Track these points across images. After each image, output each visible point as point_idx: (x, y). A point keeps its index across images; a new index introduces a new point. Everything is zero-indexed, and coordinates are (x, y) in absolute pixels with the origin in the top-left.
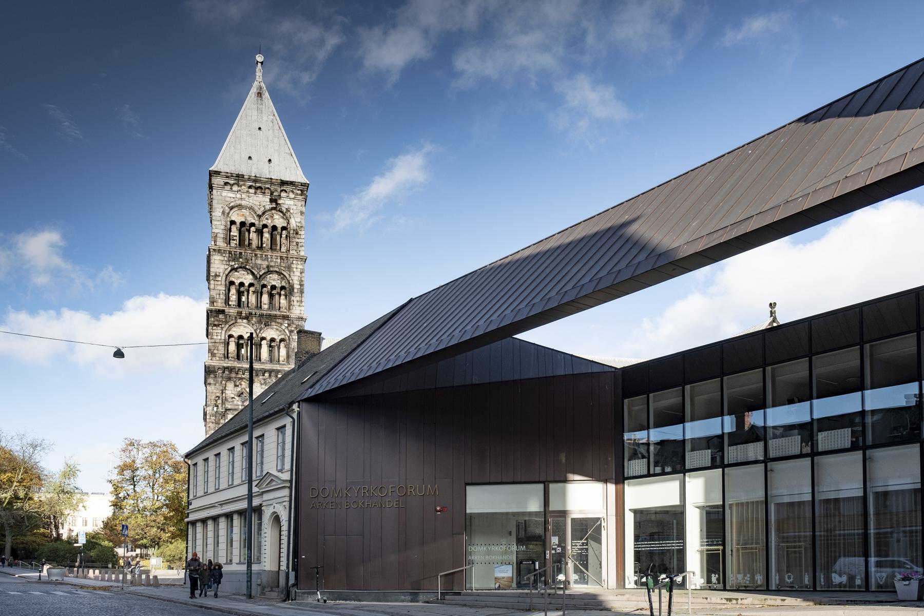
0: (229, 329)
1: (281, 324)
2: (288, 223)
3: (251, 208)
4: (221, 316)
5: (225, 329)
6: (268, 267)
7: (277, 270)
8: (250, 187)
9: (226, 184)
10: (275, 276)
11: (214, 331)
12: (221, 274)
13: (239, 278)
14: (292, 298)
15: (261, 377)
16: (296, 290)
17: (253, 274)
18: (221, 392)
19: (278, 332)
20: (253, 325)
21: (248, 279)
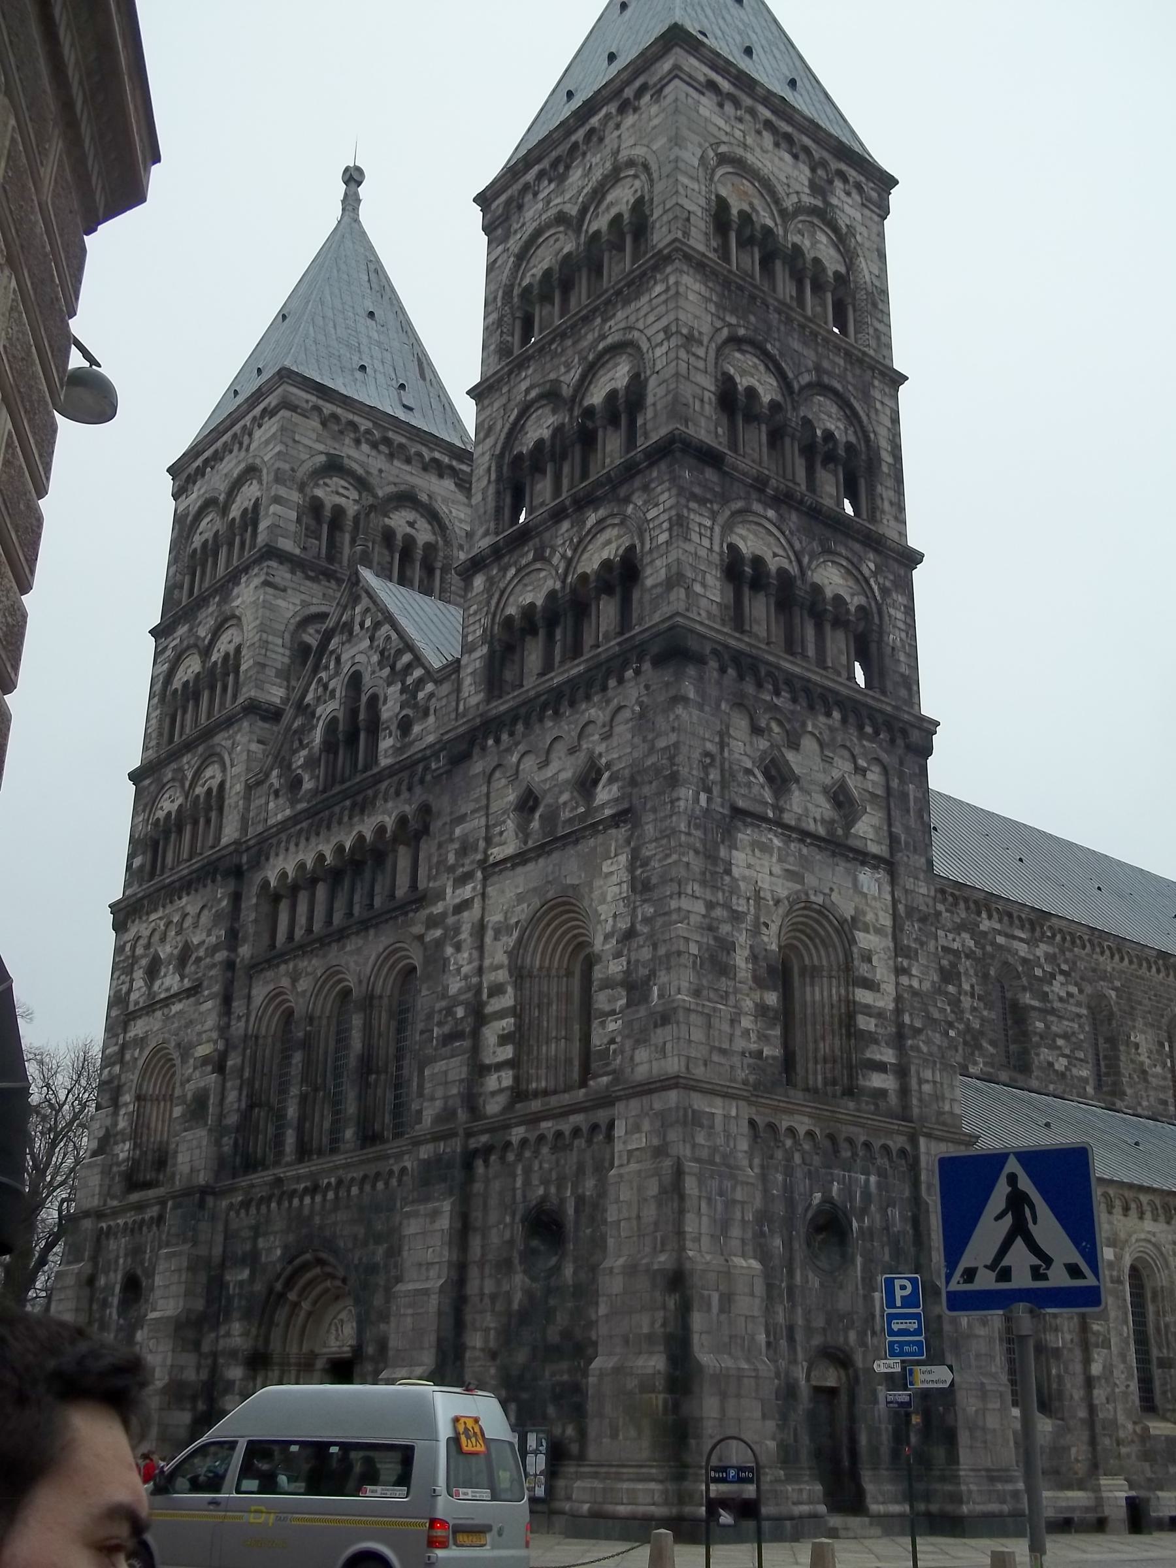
0: (728, 528)
1: (860, 559)
2: (850, 265)
3: (766, 186)
4: (710, 474)
5: (721, 520)
6: (818, 368)
7: (839, 387)
8: (768, 124)
9: (712, 85)
10: (834, 409)
11: (692, 516)
12: (705, 340)
13: (743, 373)
14: (879, 489)
15: (822, 719)
16: (885, 469)
17: (781, 375)
18: (717, 739)
19: (851, 583)
20: (791, 532)
21: (767, 390)
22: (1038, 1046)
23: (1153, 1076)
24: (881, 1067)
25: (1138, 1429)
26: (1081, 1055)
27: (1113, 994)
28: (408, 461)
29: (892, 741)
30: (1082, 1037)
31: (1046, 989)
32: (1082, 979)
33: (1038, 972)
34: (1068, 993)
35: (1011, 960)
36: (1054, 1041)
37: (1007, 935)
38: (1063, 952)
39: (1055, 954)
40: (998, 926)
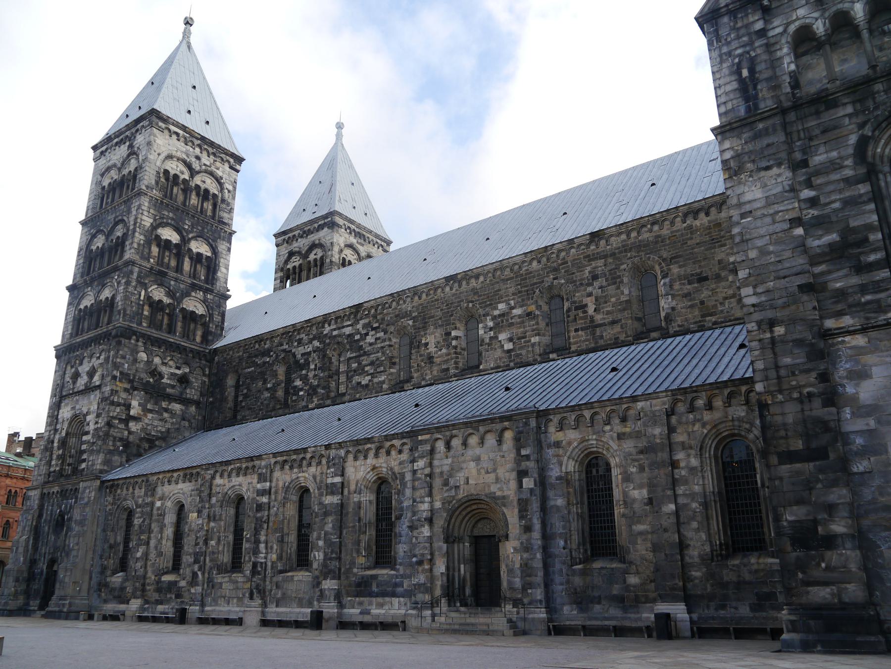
1: (113, 278)
6: (114, 220)
7: (120, 218)
8: (117, 144)
10: (120, 227)
19: (111, 289)
22: (352, 376)
23: (437, 358)
24: (84, 460)
25: (157, 578)
26: (382, 369)
27: (411, 322)
28: (312, 233)
29: (108, 339)
30: (384, 358)
31: (361, 344)
32: (387, 325)
33: (357, 337)
34: (377, 339)
35: (340, 339)
36: (363, 369)
37: (339, 328)
38: (375, 317)
39: (370, 322)
40: (334, 327)
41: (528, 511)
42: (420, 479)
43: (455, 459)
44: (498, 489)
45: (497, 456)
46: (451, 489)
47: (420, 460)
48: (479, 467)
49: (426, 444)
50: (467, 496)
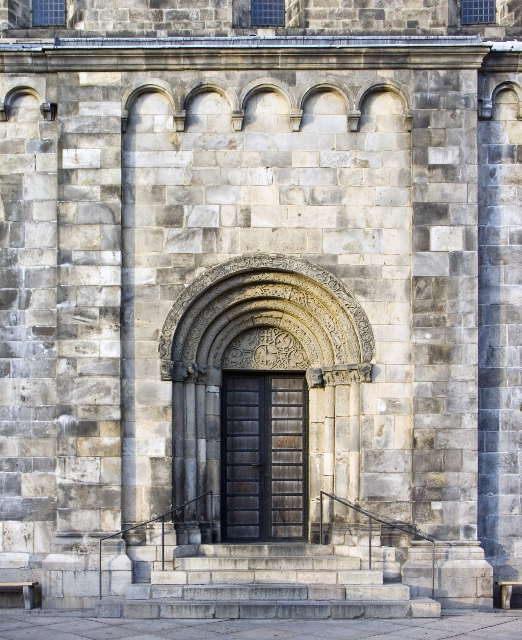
41: (441, 310)
42: (83, 196)
43: (207, 156)
44: (347, 247)
45: (343, 160)
46: (191, 234)
47: (84, 143)
48: (286, 185)
49: (106, 97)
50: (245, 258)
